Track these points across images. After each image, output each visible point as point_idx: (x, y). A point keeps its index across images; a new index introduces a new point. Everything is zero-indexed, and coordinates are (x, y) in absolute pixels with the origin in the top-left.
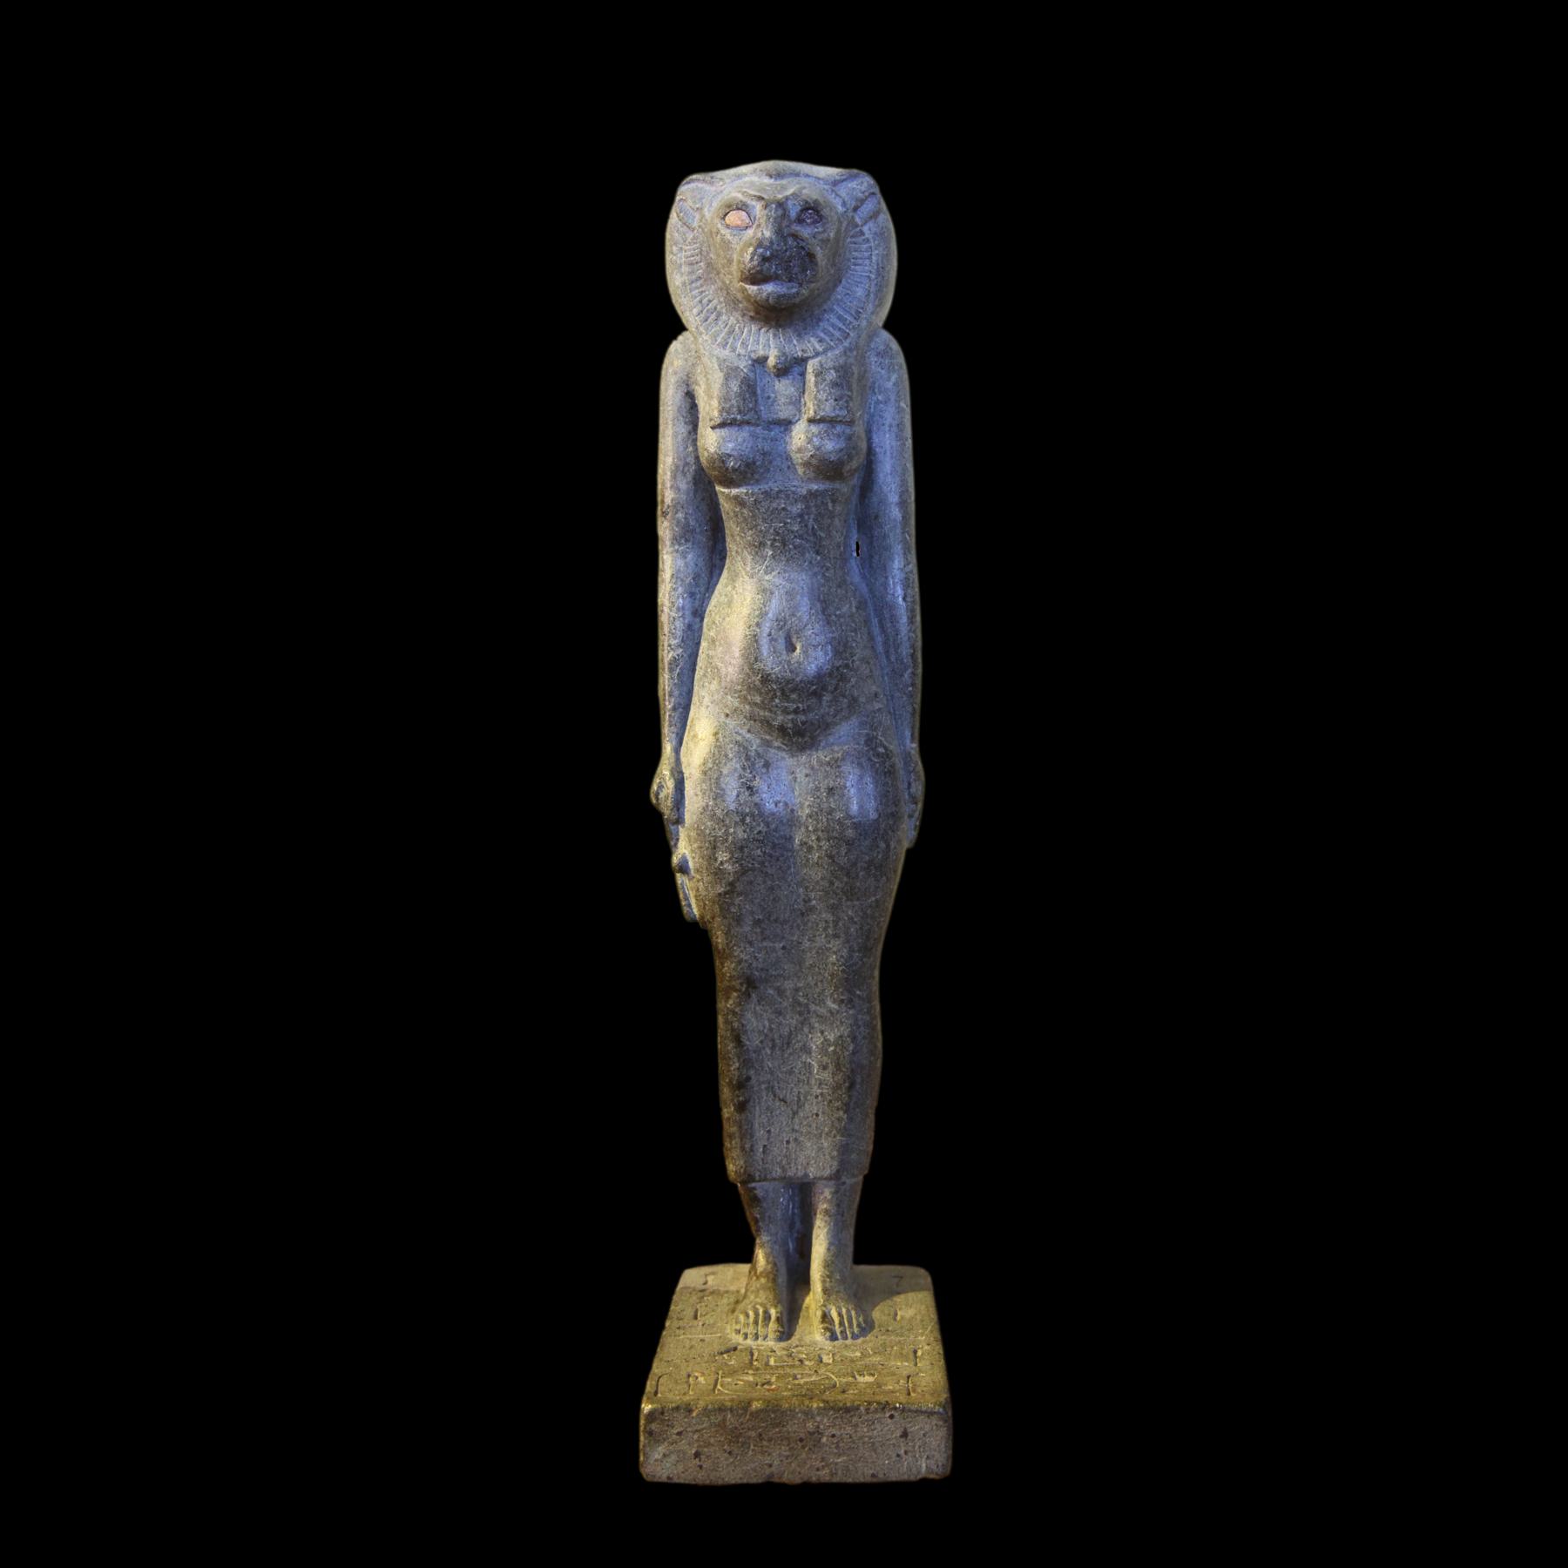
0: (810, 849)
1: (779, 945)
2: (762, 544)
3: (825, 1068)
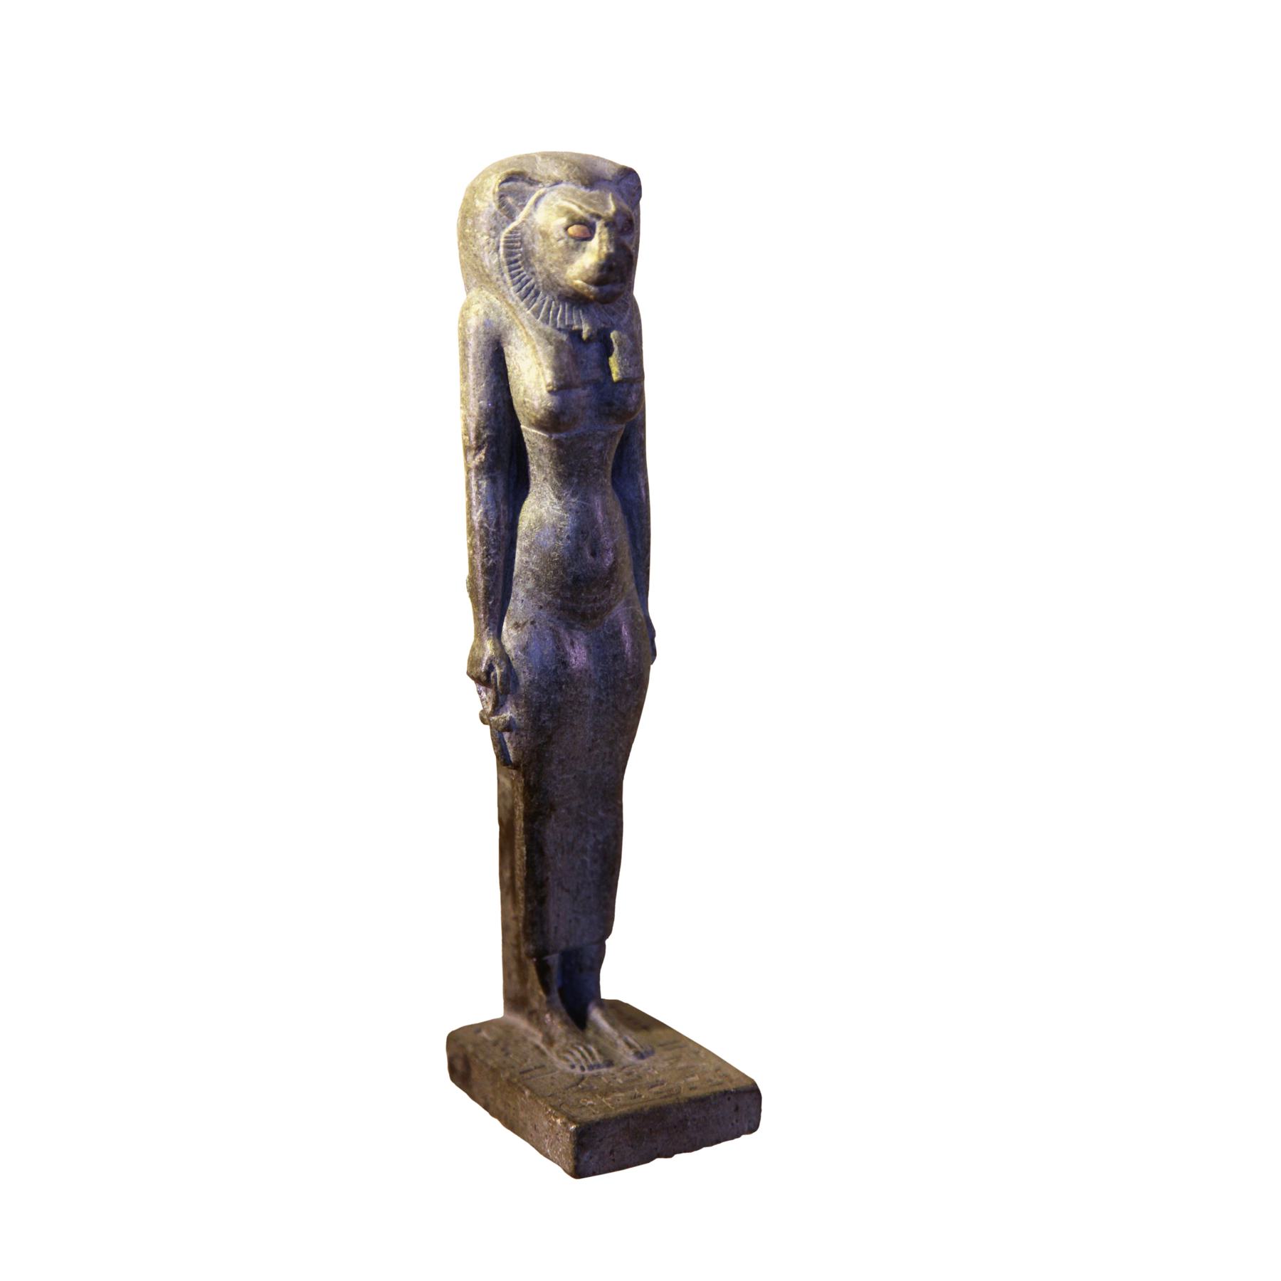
0: (601, 702)
1: (571, 776)
2: (571, 475)
3: (595, 861)
